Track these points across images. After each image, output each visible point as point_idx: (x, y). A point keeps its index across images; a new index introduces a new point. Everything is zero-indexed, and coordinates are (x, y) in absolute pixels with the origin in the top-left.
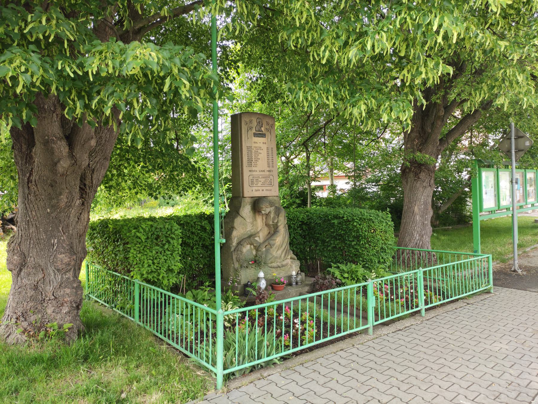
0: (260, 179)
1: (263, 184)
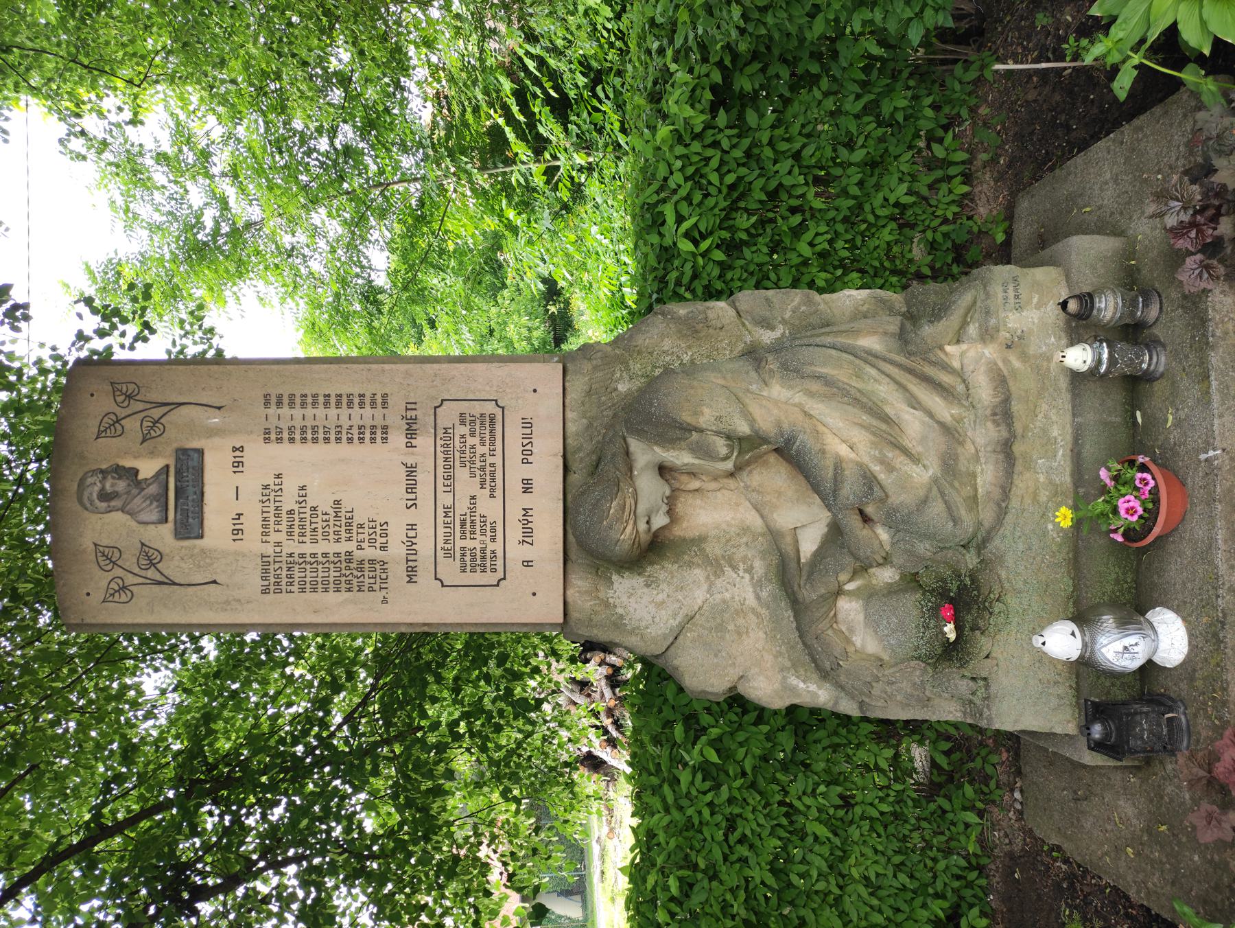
0: (462, 507)
1: (489, 479)
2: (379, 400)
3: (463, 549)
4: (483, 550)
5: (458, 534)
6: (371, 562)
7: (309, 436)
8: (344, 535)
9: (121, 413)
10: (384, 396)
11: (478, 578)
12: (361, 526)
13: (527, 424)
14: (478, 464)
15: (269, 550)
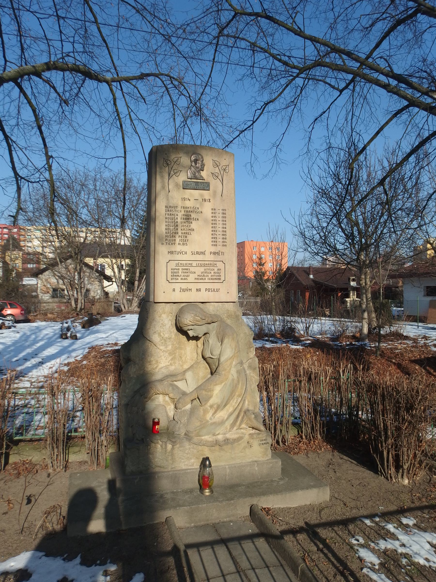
0: (192, 269)
1: (200, 278)
2: (225, 244)
3: (179, 269)
4: (178, 276)
5: (183, 268)
6: (175, 240)
7: (214, 222)
8: (183, 232)
9: (220, 167)
10: (226, 245)
11: (170, 274)
12: (186, 237)
13: (218, 290)
14: (205, 274)
15: (179, 209)
